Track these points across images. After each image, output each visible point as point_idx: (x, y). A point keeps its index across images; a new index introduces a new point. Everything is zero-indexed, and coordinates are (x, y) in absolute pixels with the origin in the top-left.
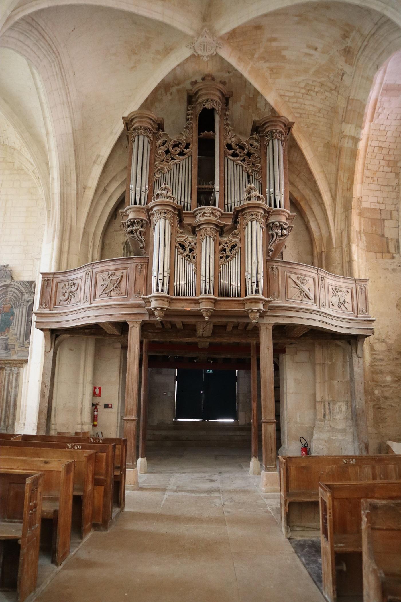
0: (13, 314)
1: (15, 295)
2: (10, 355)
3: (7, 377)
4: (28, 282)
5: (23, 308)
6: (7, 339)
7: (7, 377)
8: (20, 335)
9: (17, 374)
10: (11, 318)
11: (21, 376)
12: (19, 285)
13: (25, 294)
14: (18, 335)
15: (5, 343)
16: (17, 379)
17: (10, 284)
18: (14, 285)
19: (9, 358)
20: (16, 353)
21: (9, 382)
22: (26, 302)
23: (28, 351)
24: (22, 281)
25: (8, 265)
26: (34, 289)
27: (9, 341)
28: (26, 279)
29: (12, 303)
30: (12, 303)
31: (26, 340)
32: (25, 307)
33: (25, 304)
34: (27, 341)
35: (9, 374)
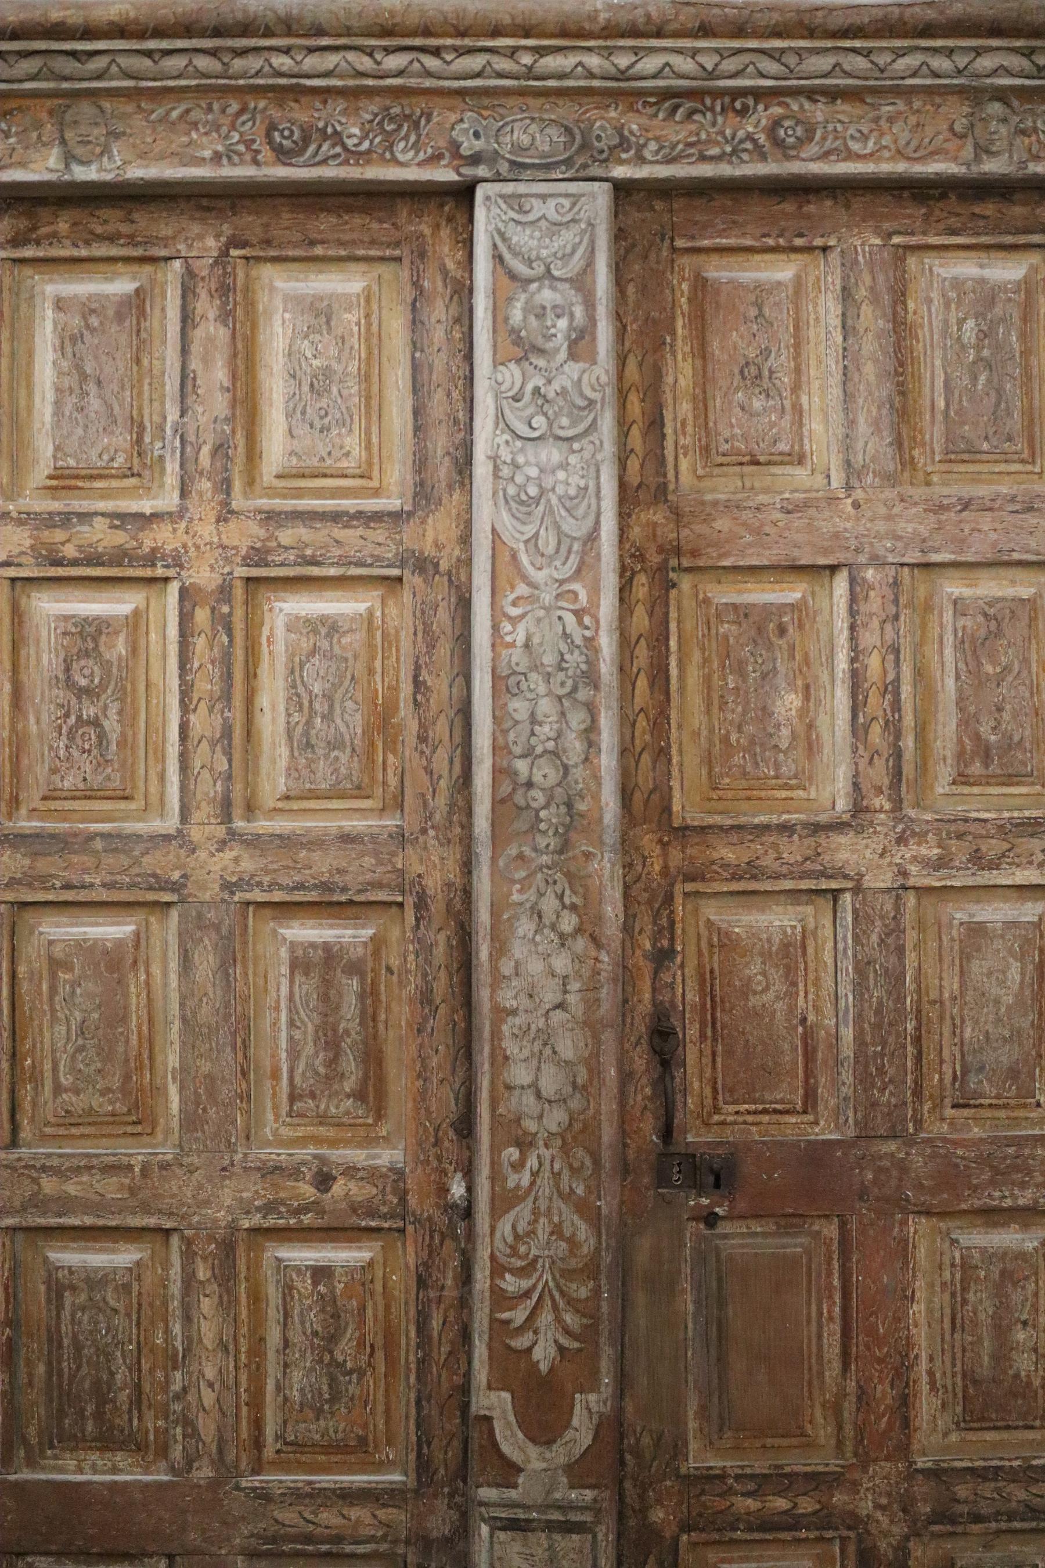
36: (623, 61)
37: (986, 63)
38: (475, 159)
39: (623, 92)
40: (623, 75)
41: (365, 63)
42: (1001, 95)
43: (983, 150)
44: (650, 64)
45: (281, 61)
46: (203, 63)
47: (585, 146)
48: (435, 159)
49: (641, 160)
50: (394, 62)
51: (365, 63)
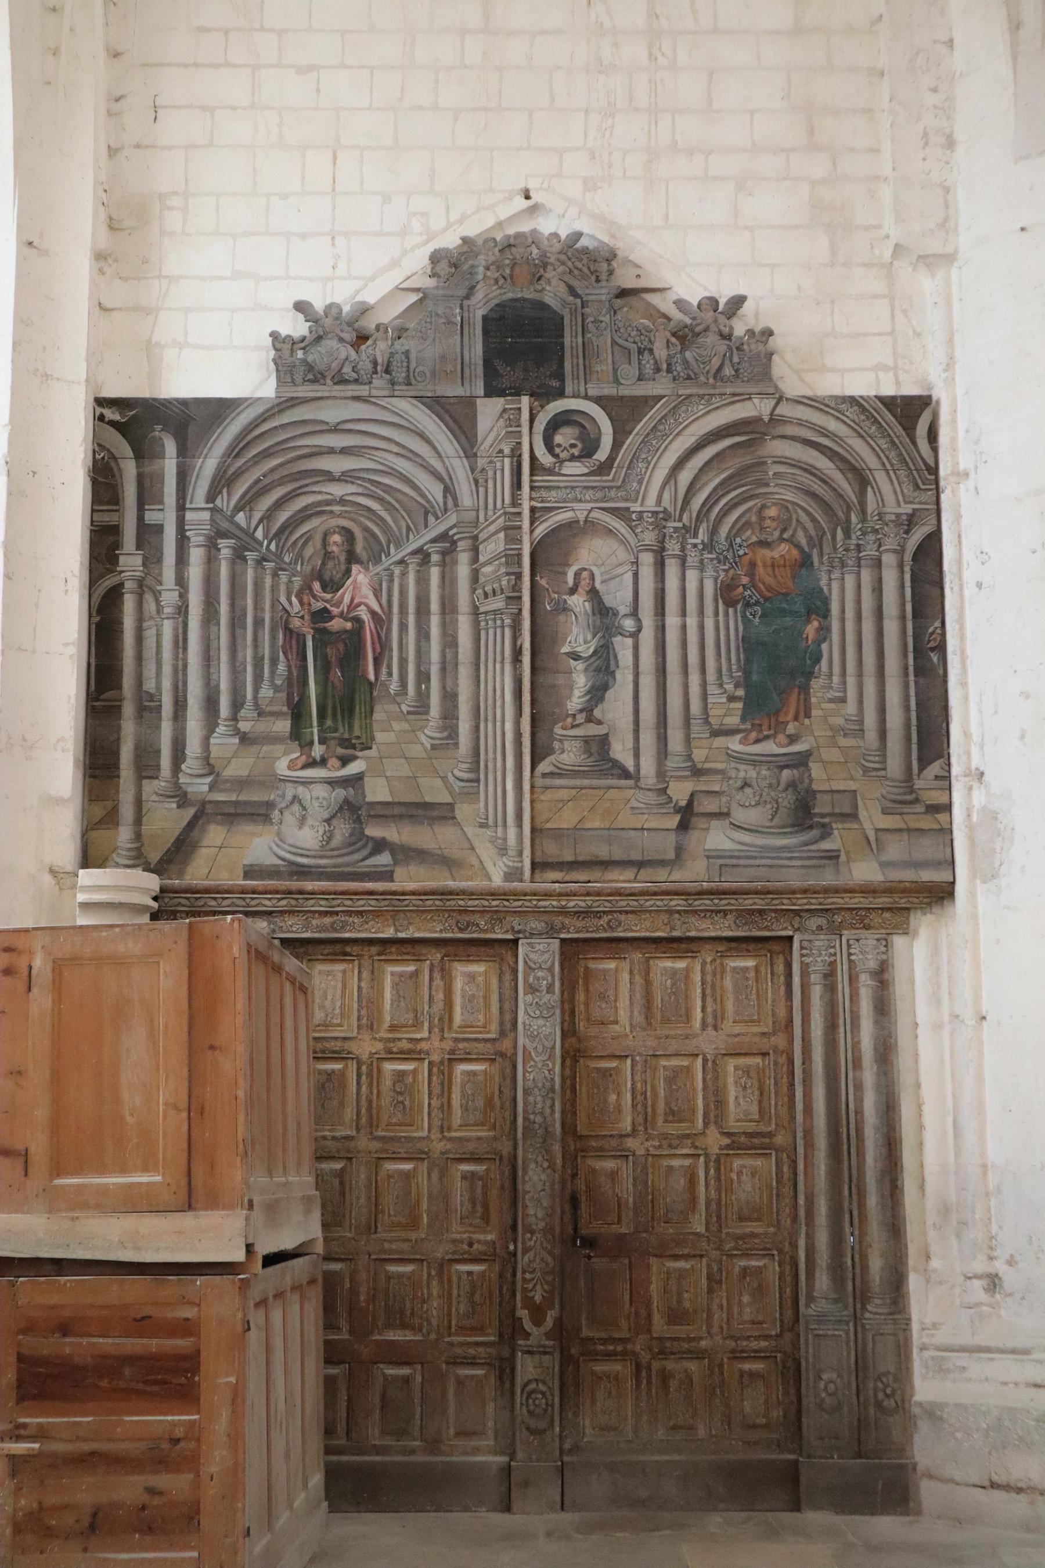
0: (817, 606)
1: (818, 487)
2: (833, 856)
3: (817, 991)
4: (889, 403)
5: (878, 564)
6: (801, 761)
7: (817, 991)
8: (883, 733)
9: (882, 976)
10: (811, 630)
11: (899, 989)
12: (833, 425)
13: (880, 477)
15: (792, 785)
16: (883, 1008)
17: (775, 420)
18: (801, 423)
19: (828, 878)
20: (873, 845)
21: (831, 1027)
23: (947, 832)
24: (852, 400)
25: (737, 302)
26: (935, 450)
27: (816, 770)
28: (861, 386)
29: (803, 541)
30: (803, 541)
31: (924, 762)
32: (889, 560)
33: (890, 543)
34: (935, 768)
35: (830, 975)
36: (564, 903)
37: (673, 903)
38: (519, 932)
39: (564, 912)
40: (563, 907)
41: (486, 903)
42: (678, 912)
43: (673, 929)
44: (572, 904)
45: (461, 903)
46: (437, 903)
47: (552, 928)
48: (507, 932)
49: (569, 932)
50: (494, 903)
51: (486, 903)
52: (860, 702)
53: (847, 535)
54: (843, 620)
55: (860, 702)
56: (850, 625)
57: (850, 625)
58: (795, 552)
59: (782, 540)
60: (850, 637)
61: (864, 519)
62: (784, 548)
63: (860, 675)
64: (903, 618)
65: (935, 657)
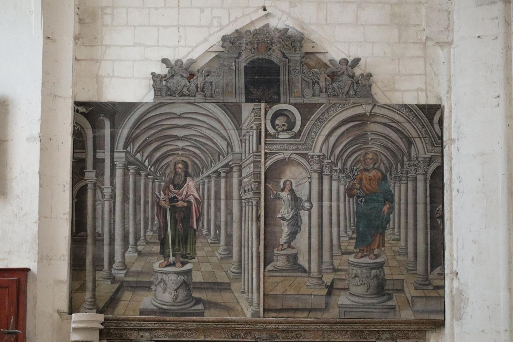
0: (389, 198)
1: (390, 145)
2: (393, 308)
4: (422, 107)
5: (415, 180)
6: (380, 266)
10: (386, 208)
12: (397, 117)
13: (418, 141)
14: (411, 255)
15: (376, 276)
17: (372, 115)
18: (383, 116)
19: (390, 317)
20: (410, 303)
22: (421, 165)
24: (406, 106)
25: (357, 61)
27: (387, 270)
28: (411, 99)
30: (382, 168)
31: (433, 267)
32: (420, 178)
33: (421, 171)
34: (438, 270)
36: (277, 327)
37: (324, 327)
38: (258, 338)
39: (277, 330)
40: (277, 328)
41: (244, 326)
42: (326, 331)
43: (324, 338)
44: (280, 327)
45: (233, 326)
46: (223, 326)
47: (272, 337)
48: (252, 338)
49: (279, 339)
50: (247, 326)
51: (244, 326)
52: (406, 240)
53: (402, 166)
54: (400, 204)
55: (406, 240)
56: (403, 207)
57: (403, 207)
58: (380, 174)
59: (374, 168)
60: (403, 212)
61: (410, 159)
62: (375, 172)
63: (406, 228)
64: (426, 203)
65: (439, 221)
